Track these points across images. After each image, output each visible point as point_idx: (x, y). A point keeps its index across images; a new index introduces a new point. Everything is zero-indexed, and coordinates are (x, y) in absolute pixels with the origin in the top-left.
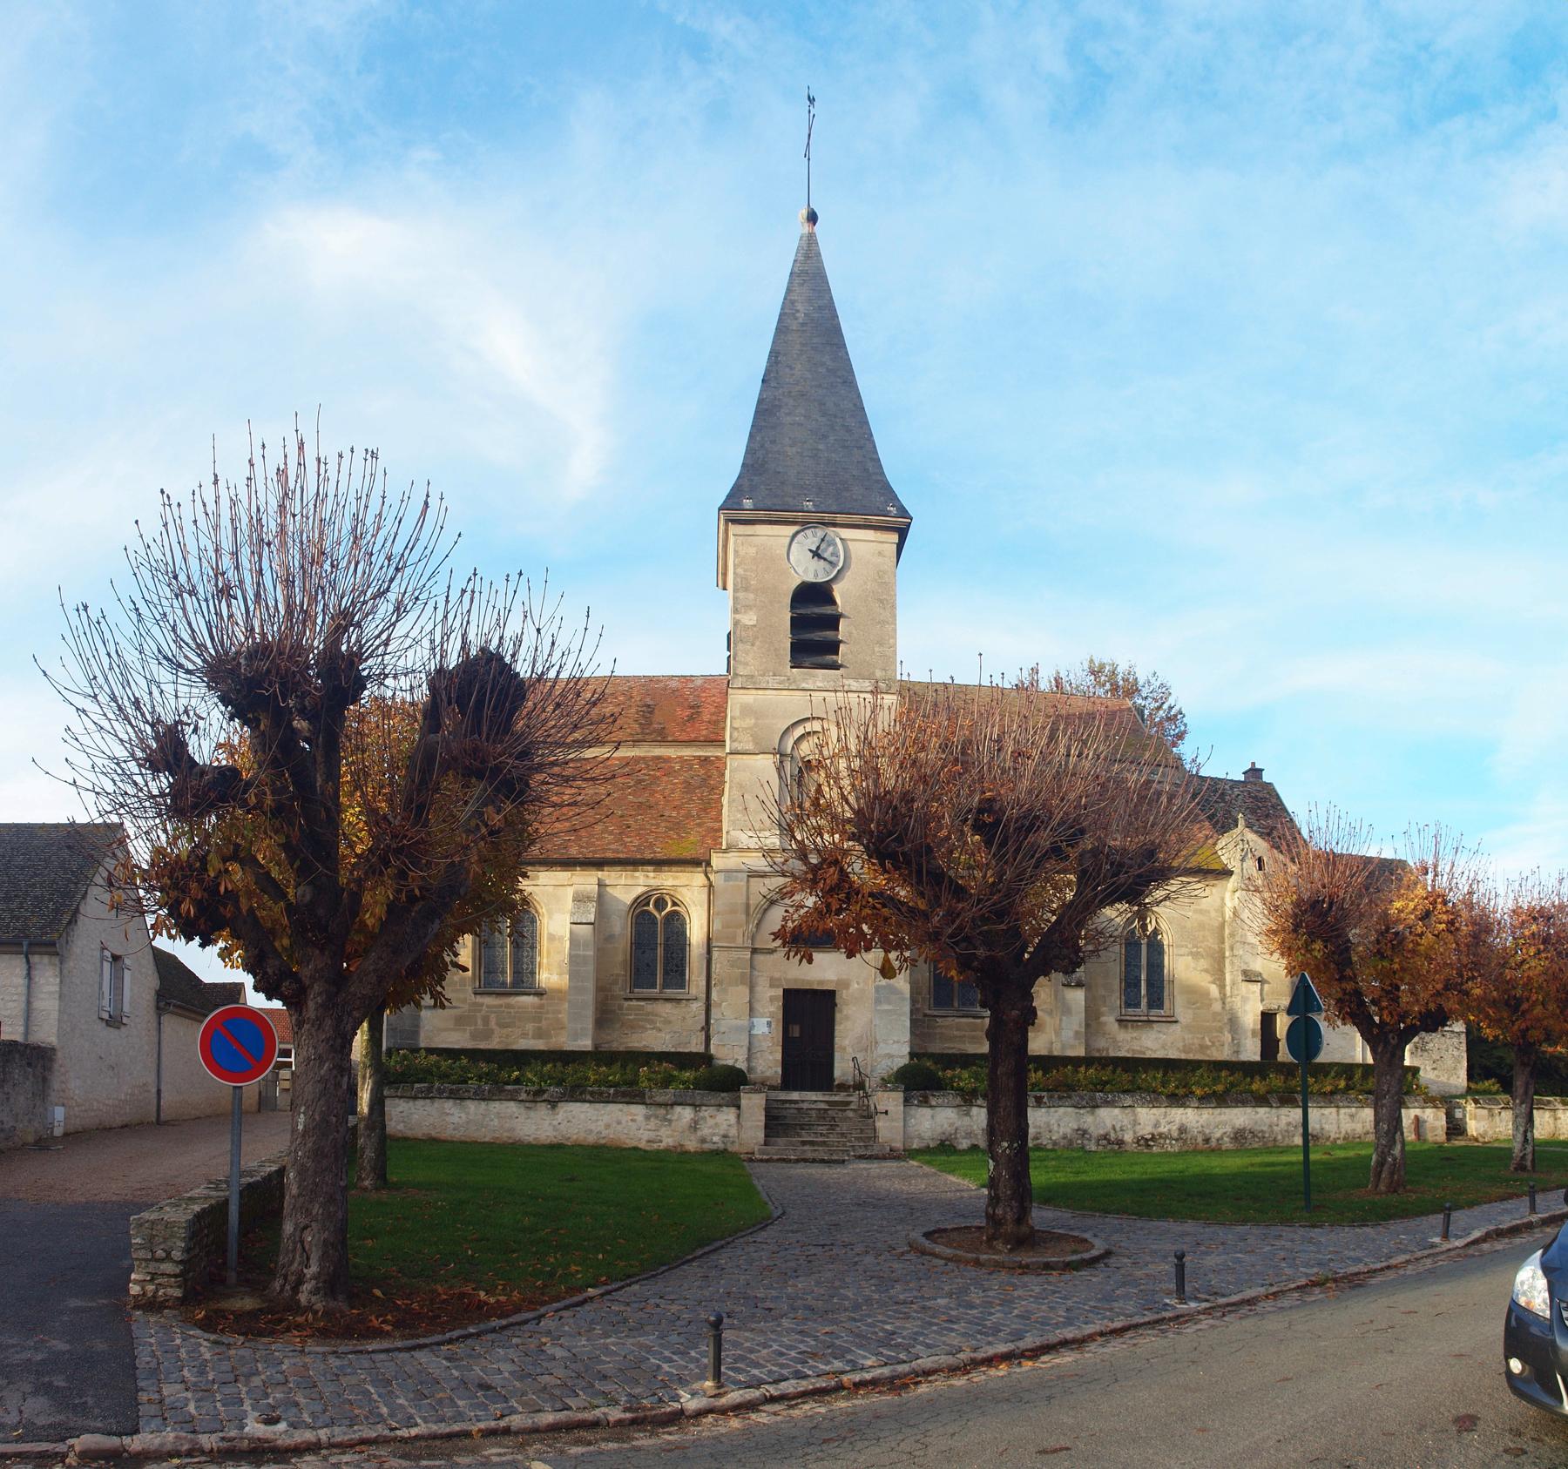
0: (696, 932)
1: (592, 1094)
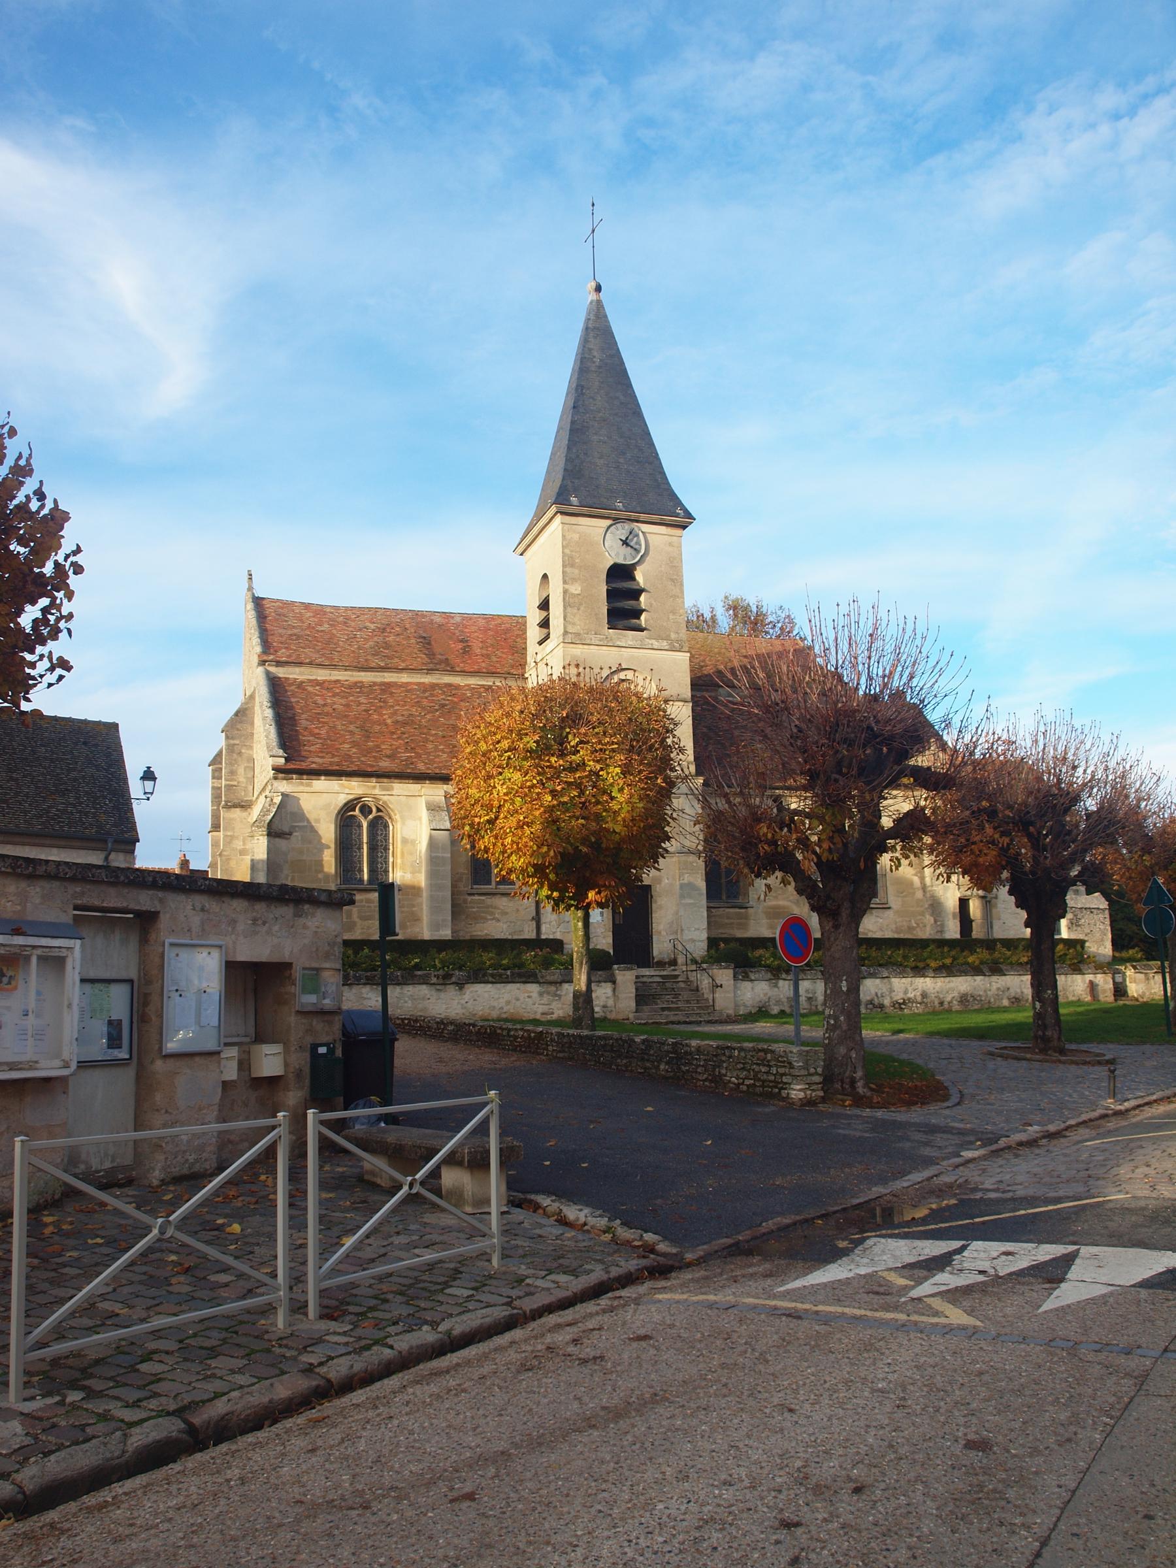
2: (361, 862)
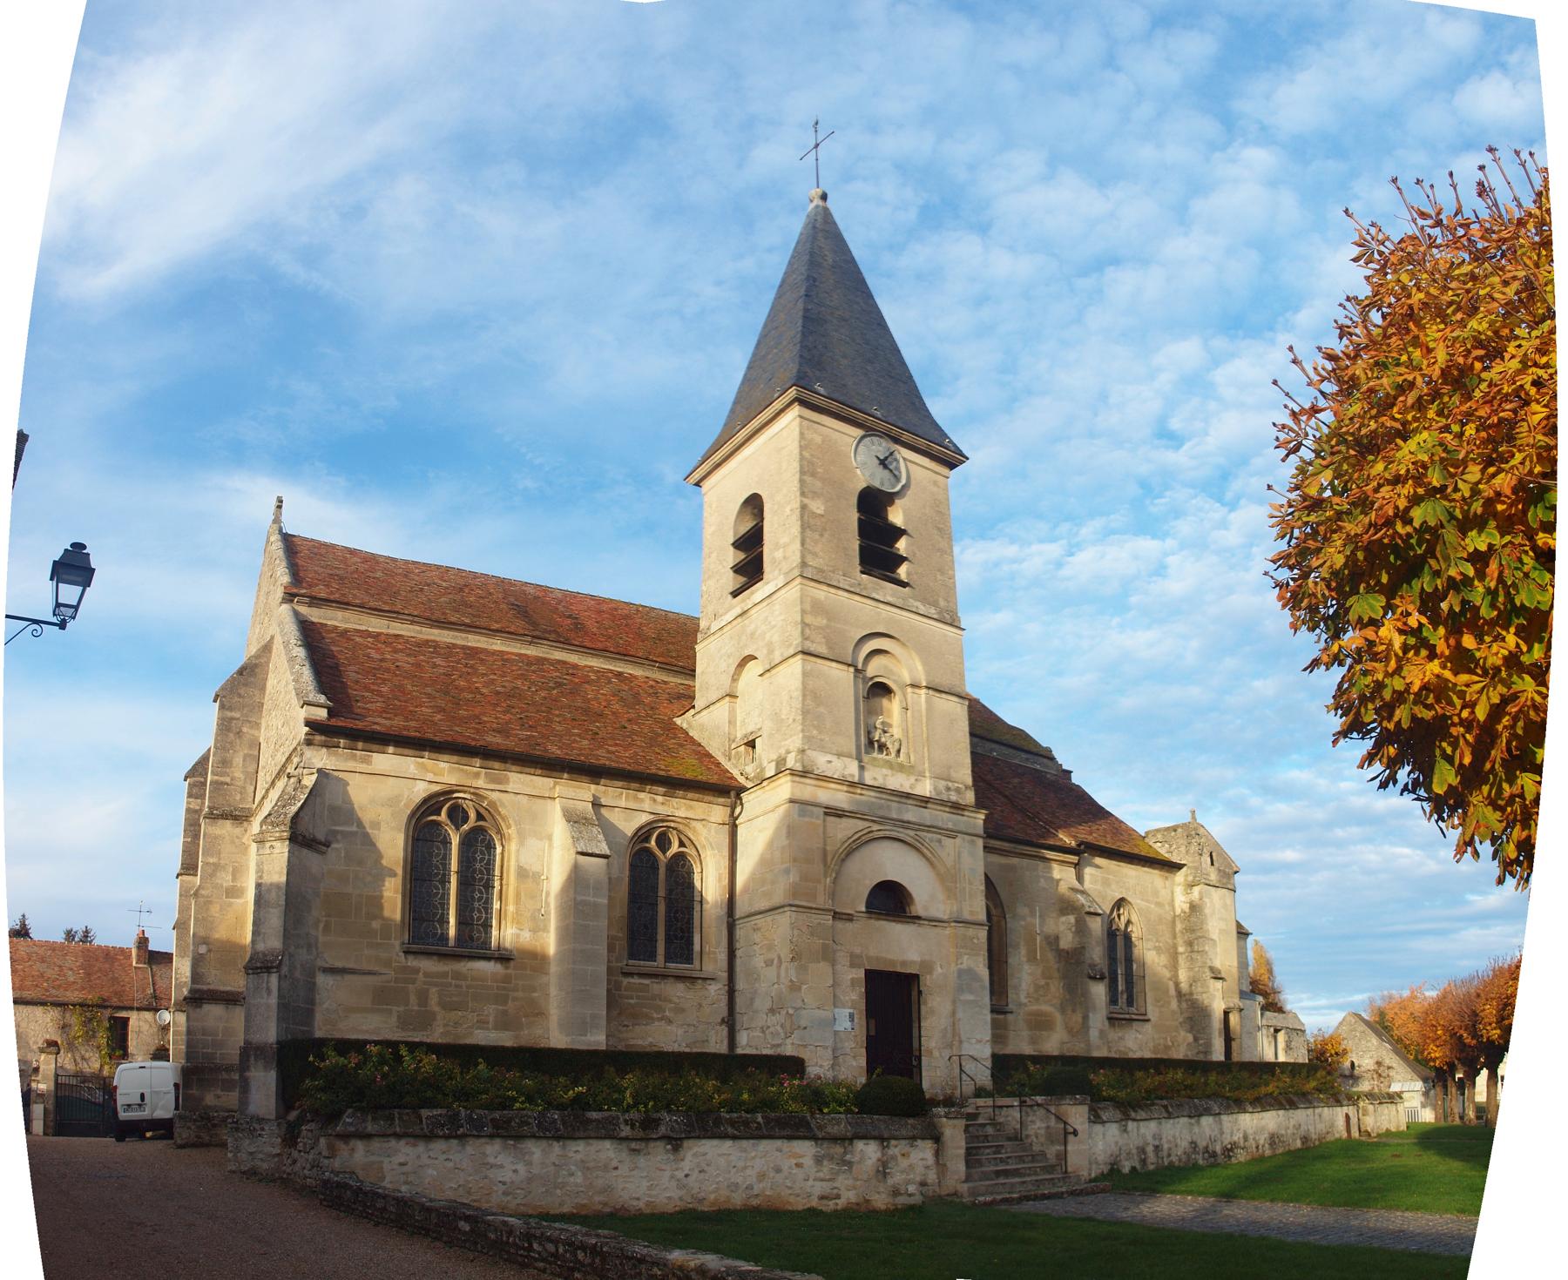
1: (732, 1123)
2: (444, 905)
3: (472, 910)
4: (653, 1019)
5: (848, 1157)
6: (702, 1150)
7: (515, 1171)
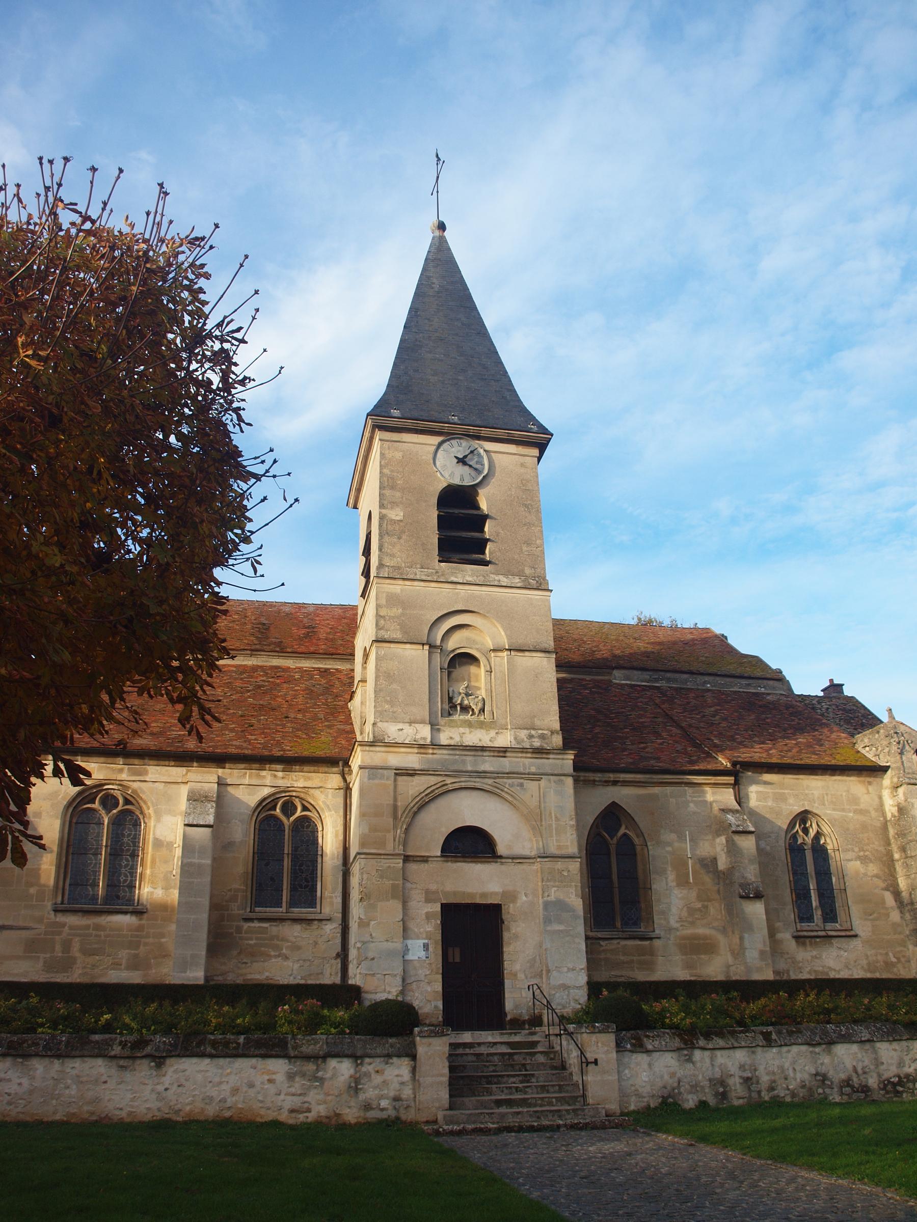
0: (329, 840)
2: (96, 873)
3: (120, 875)
4: (270, 956)
5: (320, 1074)
6: (181, 1067)
7: (20, 1084)
